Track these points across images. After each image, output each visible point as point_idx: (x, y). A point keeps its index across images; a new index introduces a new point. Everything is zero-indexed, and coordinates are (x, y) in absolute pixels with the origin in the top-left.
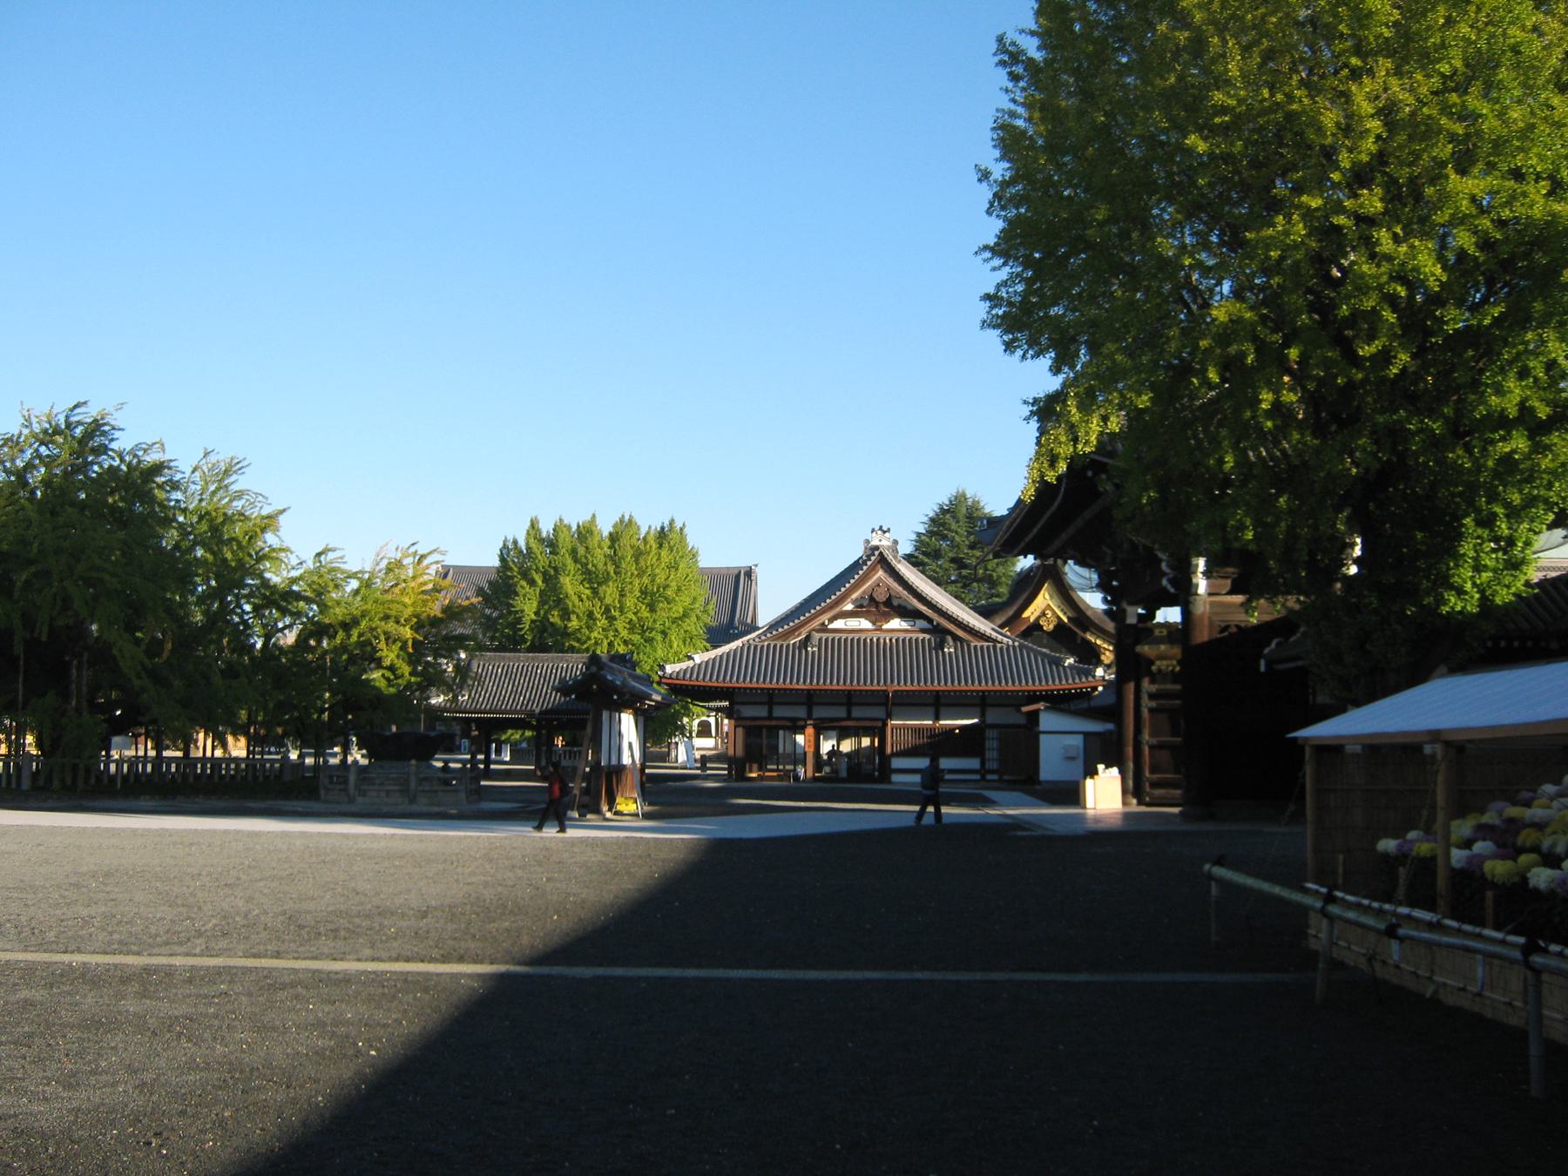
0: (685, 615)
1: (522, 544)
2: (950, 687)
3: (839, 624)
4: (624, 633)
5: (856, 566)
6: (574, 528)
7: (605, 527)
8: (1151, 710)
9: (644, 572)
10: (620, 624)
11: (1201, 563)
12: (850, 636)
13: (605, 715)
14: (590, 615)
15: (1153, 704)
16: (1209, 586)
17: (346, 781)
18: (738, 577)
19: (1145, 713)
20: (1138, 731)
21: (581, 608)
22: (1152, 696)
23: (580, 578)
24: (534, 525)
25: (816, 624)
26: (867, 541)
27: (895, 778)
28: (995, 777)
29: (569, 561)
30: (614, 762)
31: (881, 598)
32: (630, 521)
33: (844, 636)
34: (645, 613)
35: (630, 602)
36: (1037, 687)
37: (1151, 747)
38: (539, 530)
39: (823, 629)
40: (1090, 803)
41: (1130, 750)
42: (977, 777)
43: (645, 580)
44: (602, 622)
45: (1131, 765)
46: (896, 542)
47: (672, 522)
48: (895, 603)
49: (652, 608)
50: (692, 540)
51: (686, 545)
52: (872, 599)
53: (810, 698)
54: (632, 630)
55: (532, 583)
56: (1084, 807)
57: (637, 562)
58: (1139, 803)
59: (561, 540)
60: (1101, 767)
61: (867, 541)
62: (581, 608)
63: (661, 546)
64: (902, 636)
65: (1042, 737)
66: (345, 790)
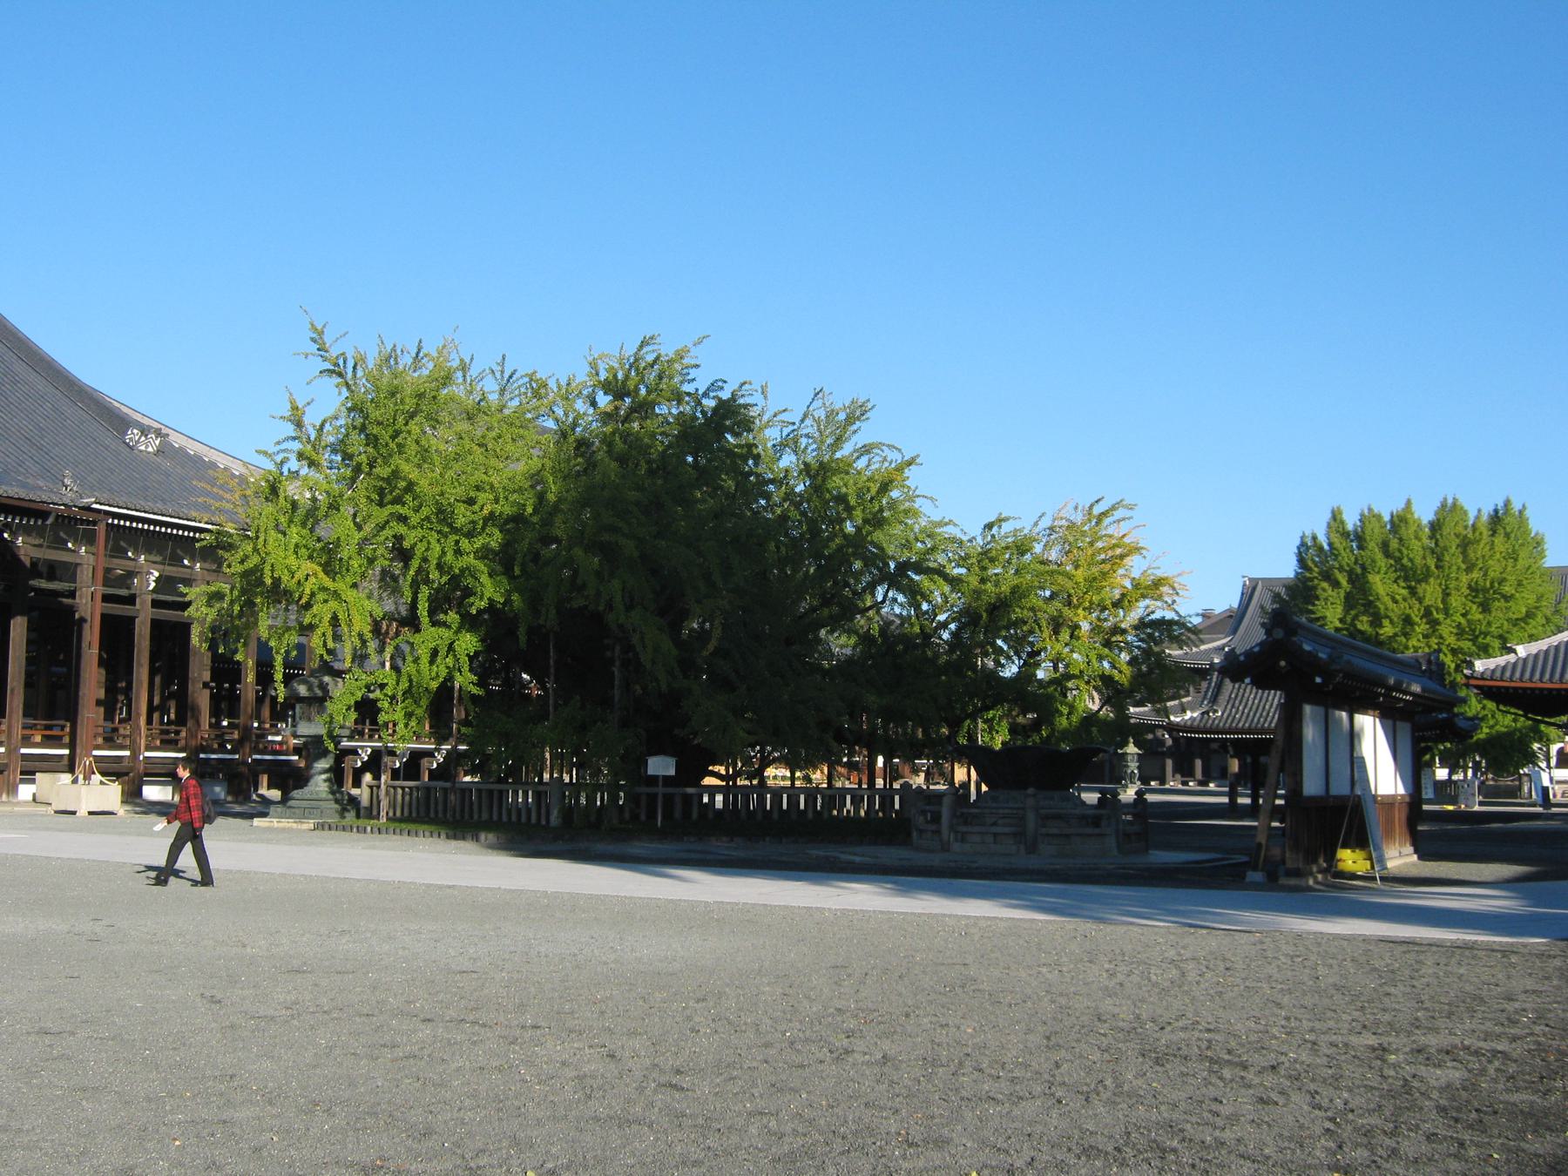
0: (1529, 615)
1: (1323, 540)
4: (1451, 640)
6: (1387, 518)
7: (1425, 513)
10: (1446, 630)
13: (1308, 709)
14: (1407, 621)
17: (936, 818)
21: (1395, 611)
23: (1394, 575)
24: (1336, 516)
29: (1379, 556)
30: (1340, 788)
32: (1454, 504)
34: (1476, 615)
35: (1456, 602)
38: (1342, 522)
43: (1475, 575)
44: (1421, 628)
47: (1507, 503)
49: (1485, 608)
50: (1535, 525)
51: (1527, 532)
54: (1460, 633)
55: (1336, 584)
57: (1464, 553)
59: (1368, 531)
62: (1395, 611)
63: (1494, 533)
66: (938, 832)
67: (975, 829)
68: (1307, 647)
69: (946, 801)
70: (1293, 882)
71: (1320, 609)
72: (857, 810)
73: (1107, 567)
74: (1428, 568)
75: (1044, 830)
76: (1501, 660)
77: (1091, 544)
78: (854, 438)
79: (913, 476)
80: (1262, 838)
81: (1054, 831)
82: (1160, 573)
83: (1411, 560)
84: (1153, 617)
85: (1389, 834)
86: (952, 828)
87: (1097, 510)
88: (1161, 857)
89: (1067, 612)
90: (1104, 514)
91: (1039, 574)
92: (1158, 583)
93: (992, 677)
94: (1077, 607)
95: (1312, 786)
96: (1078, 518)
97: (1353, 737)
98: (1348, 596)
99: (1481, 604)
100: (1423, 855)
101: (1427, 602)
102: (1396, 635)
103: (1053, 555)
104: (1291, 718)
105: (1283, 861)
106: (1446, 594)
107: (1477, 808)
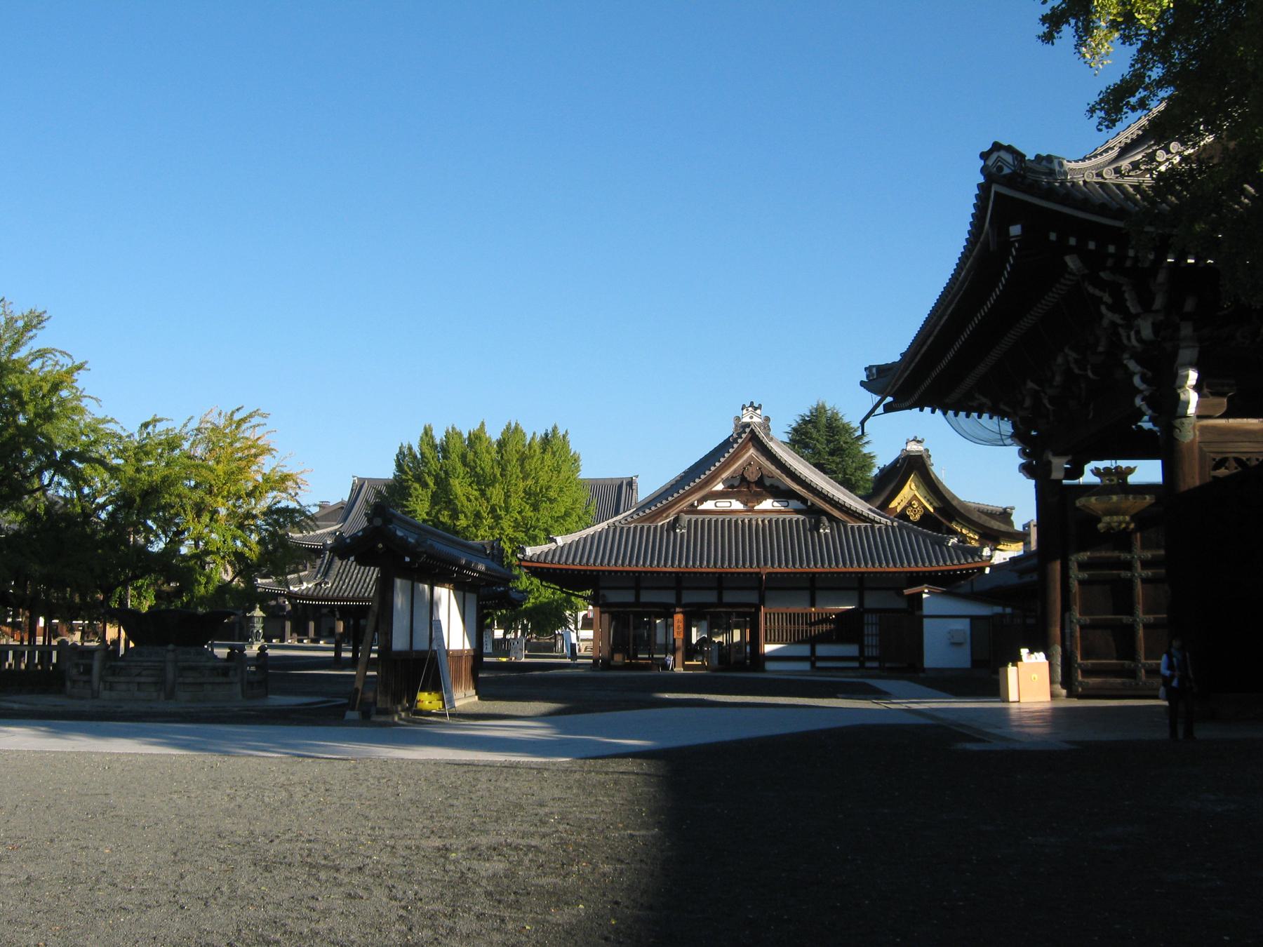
0: (567, 514)
2: (827, 569)
3: (709, 505)
4: (510, 531)
5: (727, 444)
6: (466, 435)
7: (494, 433)
8: (1081, 582)
9: (529, 475)
10: (506, 523)
11: (1193, 376)
12: (721, 518)
13: (398, 582)
14: (478, 515)
15: (1084, 575)
16: (1199, 405)
17: (88, 670)
18: (620, 487)
19: (1075, 586)
20: (1066, 607)
21: (469, 508)
22: (1082, 566)
24: (427, 432)
25: (684, 505)
26: (738, 419)
27: (770, 666)
28: (875, 664)
29: (459, 465)
30: (421, 644)
31: (752, 476)
32: (516, 428)
33: (714, 518)
35: (514, 502)
36: (921, 568)
37: (1082, 627)
38: (432, 437)
39: (692, 510)
40: (1013, 696)
41: (1057, 631)
42: (856, 664)
43: (530, 482)
44: (488, 521)
45: (1059, 649)
46: (767, 419)
47: (555, 429)
48: (768, 482)
49: (535, 508)
50: (574, 446)
51: (568, 452)
52: (743, 479)
53: (679, 582)
54: (516, 526)
56: (1008, 701)
57: (522, 465)
58: (1069, 695)
59: (451, 446)
60: (1024, 652)
61: (738, 419)
62: (469, 508)
63: (544, 451)
64: (774, 517)
65: (926, 621)
66: (89, 682)
67: (122, 679)
68: (399, 533)
69: (97, 656)
70: (382, 719)
71: (412, 504)
72: (18, 662)
73: (243, 463)
74: (495, 476)
75: (181, 680)
76: (545, 547)
77: (231, 444)
78: (31, 343)
79: (81, 379)
80: (359, 685)
81: (187, 681)
82: (286, 471)
83: (482, 469)
84: (279, 506)
85: (457, 680)
86: (101, 678)
87: (237, 417)
88: (277, 701)
89: (208, 499)
90: (243, 420)
91: (186, 467)
92: (284, 478)
93: (142, 550)
94: (216, 496)
95: (399, 643)
96: (221, 422)
97: (432, 605)
98: (434, 495)
99: (532, 505)
100: (483, 695)
101: (493, 502)
102: (468, 526)
103: (199, 451)
104: (385, 589)
105: (375, 703)
106: (507, 496)
107: (523, 660)
